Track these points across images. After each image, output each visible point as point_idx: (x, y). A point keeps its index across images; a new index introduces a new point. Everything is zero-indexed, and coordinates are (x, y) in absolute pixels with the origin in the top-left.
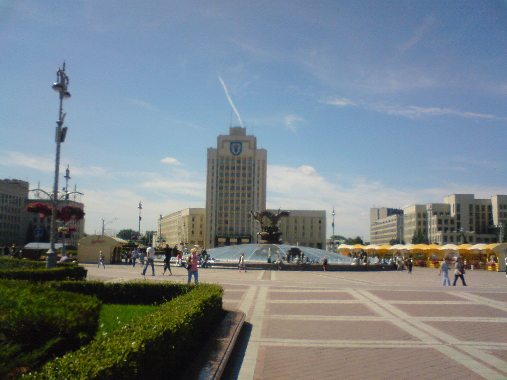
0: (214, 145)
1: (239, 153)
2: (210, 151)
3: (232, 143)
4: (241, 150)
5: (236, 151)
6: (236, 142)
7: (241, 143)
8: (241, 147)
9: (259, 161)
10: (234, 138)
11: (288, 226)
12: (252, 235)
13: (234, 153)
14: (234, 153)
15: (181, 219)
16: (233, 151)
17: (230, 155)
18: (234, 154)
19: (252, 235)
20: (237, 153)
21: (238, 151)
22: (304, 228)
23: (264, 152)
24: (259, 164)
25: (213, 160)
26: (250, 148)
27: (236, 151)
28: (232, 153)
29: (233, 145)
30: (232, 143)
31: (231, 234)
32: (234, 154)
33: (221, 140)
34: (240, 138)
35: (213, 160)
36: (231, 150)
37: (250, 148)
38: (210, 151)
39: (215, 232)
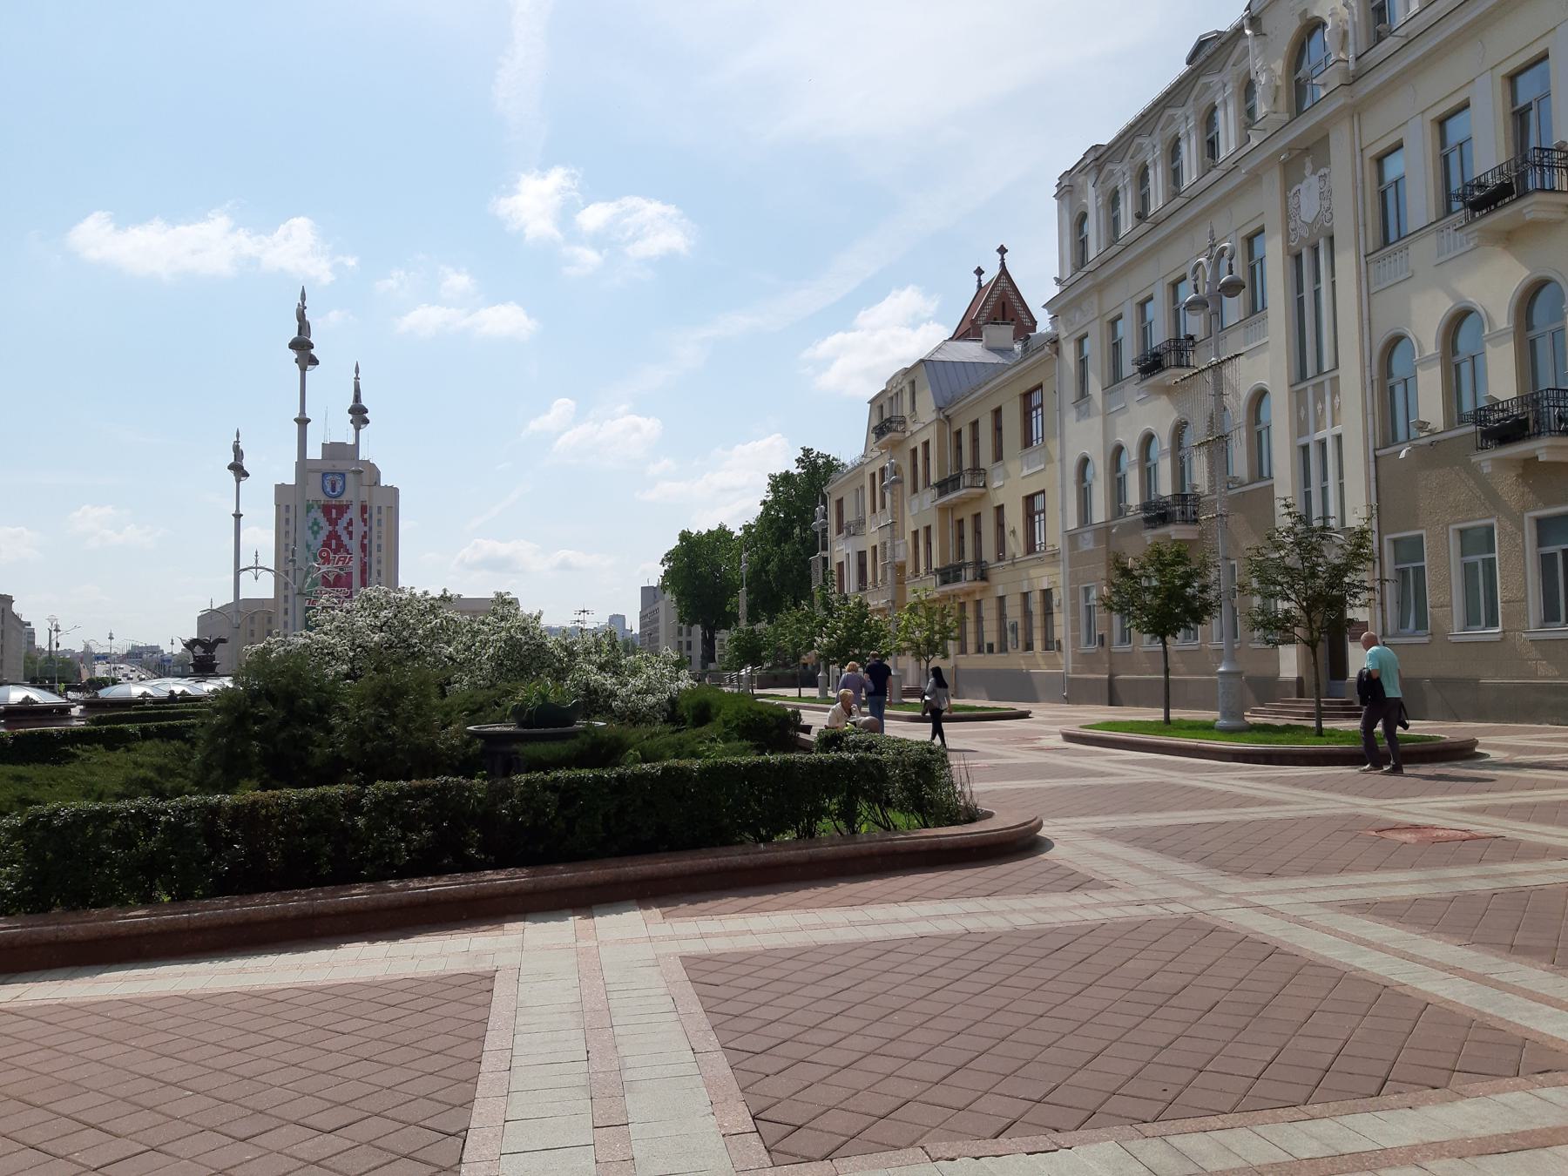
2: (280, 489)
3: (324, 475)
5: (334, 491)
7: (343, 475)
9: (379, 508)
10: (328, 467)
16: (329, 489)
21: (338, 489)
23: (394, 492)
25: (288, 507)
27: (334, 491)
29: (330, 477)
30: (324, 475)
34: (341, 466)
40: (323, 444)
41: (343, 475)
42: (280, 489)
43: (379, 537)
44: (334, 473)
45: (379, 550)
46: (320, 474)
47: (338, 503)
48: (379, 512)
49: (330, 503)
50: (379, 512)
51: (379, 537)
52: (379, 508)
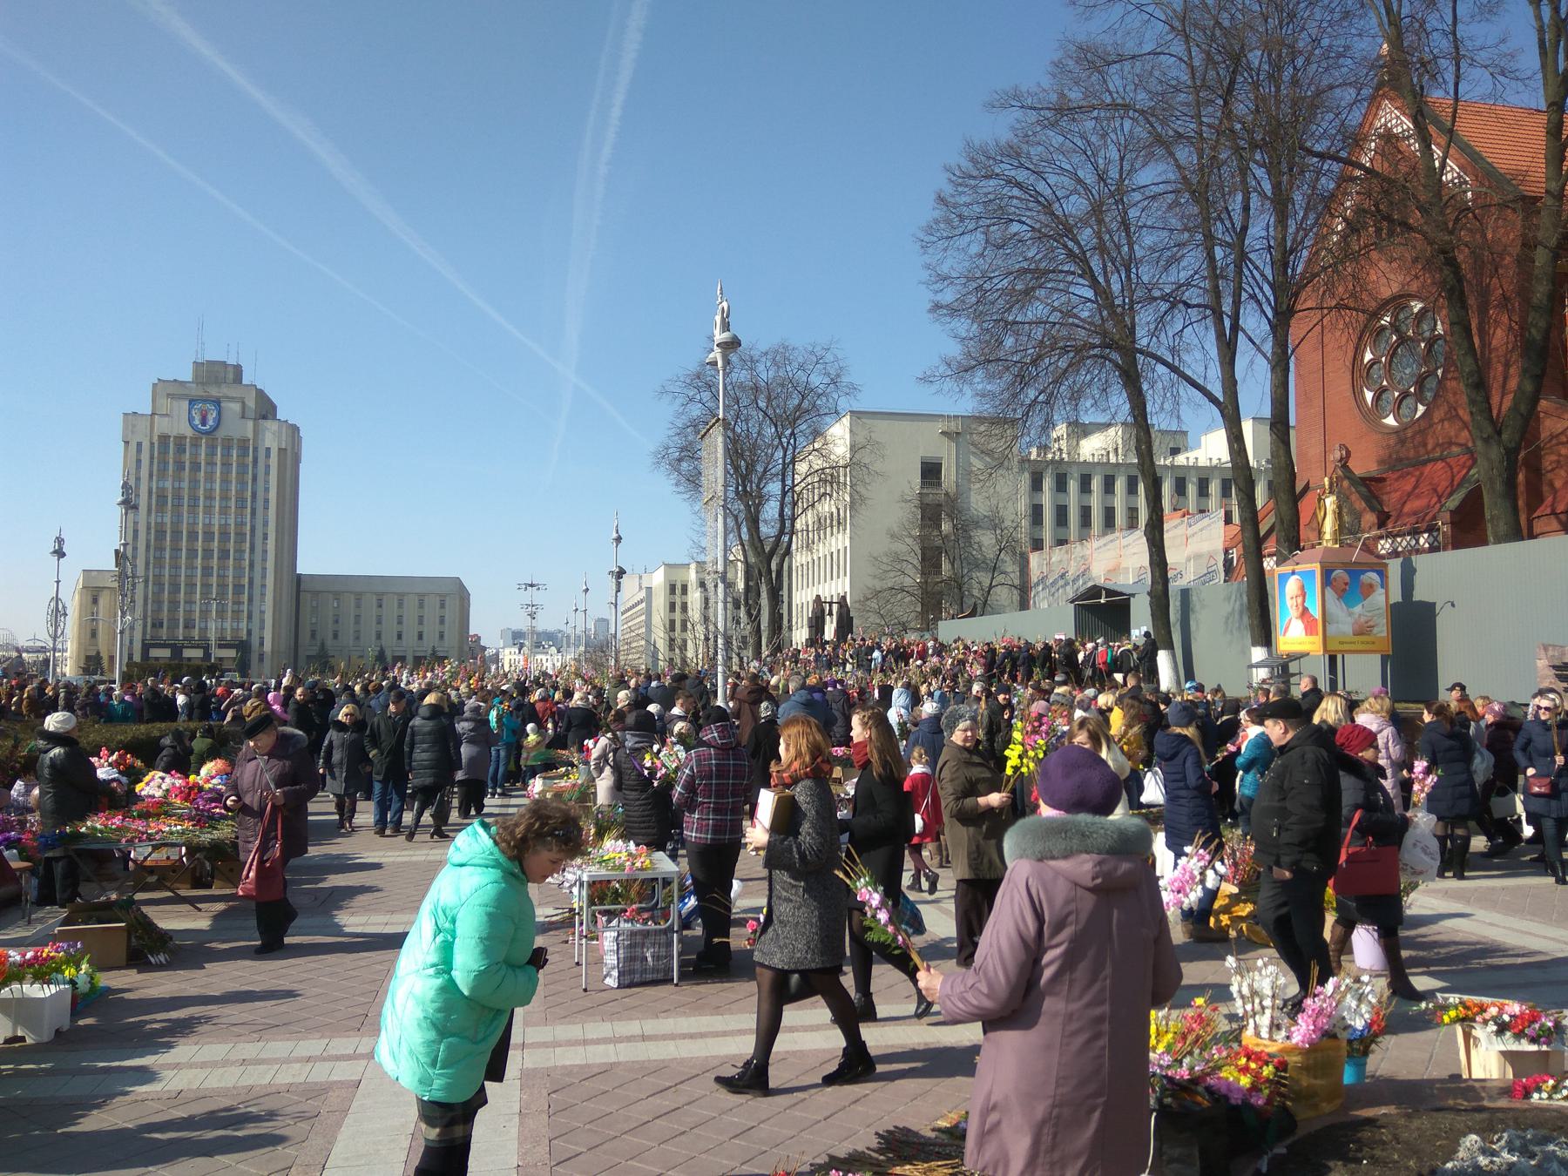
2: (131, 418)
4: (219, 420)
5: (204, 423)
6: (205, 400)
7: (217, 402)
8: (219, 413)
9: (268, 449)
10: (196, 391)
11: (358, 617)
16: (197, 422)
17: (189, 432)
18: (199, 431)
21: (211, 422)
22: (421, 620)
25: (139, 445)
26: (243, 417)
27: (204, 423)
28: (194, 427)
30: (192, 402)
31: (189, 639)
33: (166, 390)
35: (139, 445)
36: (191, 420)
37: (243, 417)
38: (131, 418)
39: (144, 633)
41: (217, 402)
46: (185, 404)
48: (268, 456)
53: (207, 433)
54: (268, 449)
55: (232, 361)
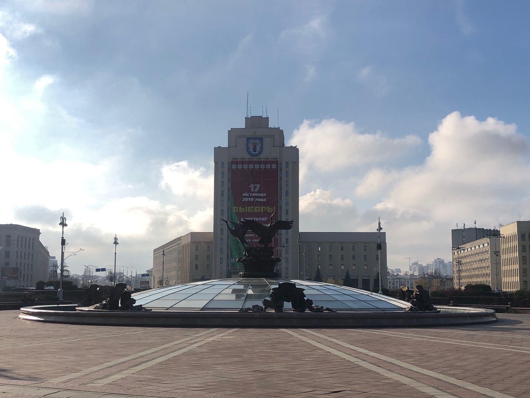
0: (225, 144)
1: (260, 153)
2: (218, 151)
3: (248, 139)
4: (262, 149)
7: (261, 139)
8: (262, 145)
12: (59, 263)
13: (253, 152)
14: (253, 152)
15: (181, 248)
16: (251, 150)
18: (252, 155)
19: (59, 263)
20: (257, 152)
21: (258, 150)
24: (287, 167)
25: (223, 163)
28: (249, 153)
30: (248, 139)
32: (252, 155)
33: (233, 134)
35: (223, 163)
40: (246, 118)
41: (261, 139)
42: (218, 151)
43: (287, 185)
44: (255, 138)
45: (287, 195)
46: (246, 139)
47: (258, 160)
49: (252, 160)
50: (287, 167)
51: (287, 185)
52: (287, 163)
53: (257, 155)
54: (287, 163)
55: (264, 116)
